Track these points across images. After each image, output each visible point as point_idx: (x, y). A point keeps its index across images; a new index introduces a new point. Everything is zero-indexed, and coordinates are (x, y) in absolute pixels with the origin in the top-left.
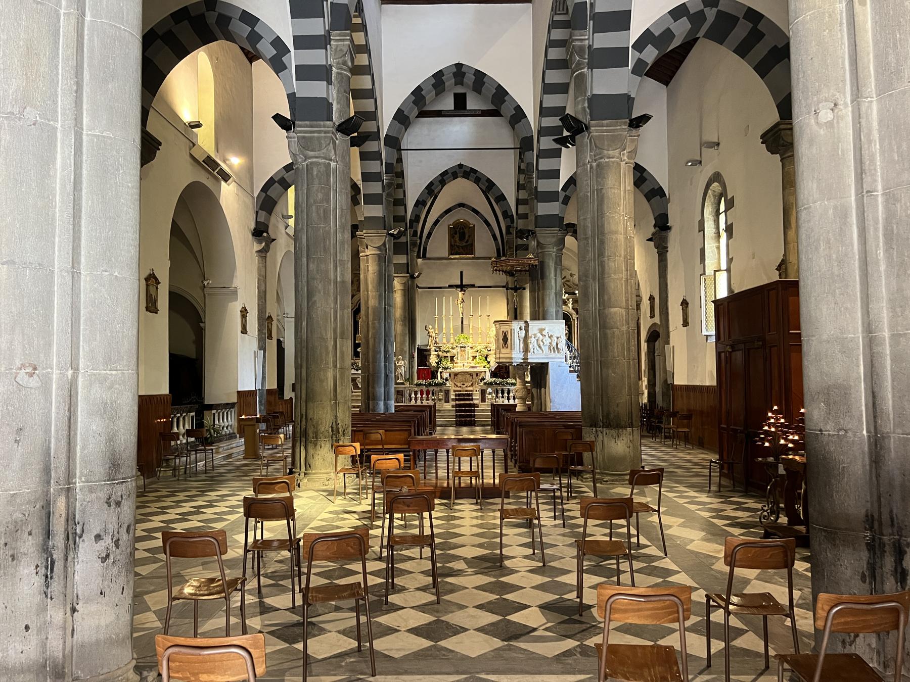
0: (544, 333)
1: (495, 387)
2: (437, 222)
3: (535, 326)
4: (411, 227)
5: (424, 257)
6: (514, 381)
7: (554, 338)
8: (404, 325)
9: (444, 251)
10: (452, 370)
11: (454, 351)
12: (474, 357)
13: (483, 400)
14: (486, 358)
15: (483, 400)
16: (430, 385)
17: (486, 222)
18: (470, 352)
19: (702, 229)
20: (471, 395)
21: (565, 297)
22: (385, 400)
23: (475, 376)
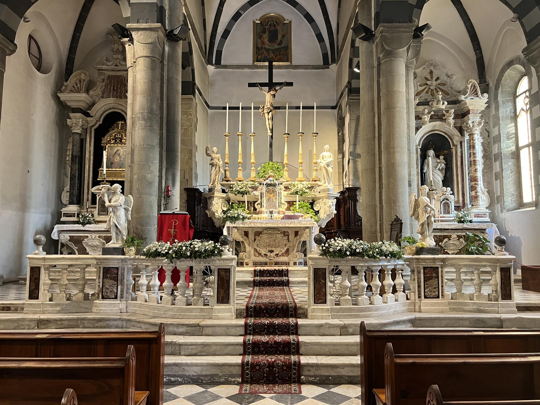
1: (352, 261)
2: (237, 16)
6: (395, 248)
8: (149, 127)
9: (248, 57)
10: (247, 224)
11: (257, 193)
12: (291, 204)
13: (320, 296)
14: (312, 204)
15: (320, 296)
16: (179, 255)
17: (309, 18)
18: (285, 196)
20: (285, 273)
21: (443, 106)
23: (292, 236)
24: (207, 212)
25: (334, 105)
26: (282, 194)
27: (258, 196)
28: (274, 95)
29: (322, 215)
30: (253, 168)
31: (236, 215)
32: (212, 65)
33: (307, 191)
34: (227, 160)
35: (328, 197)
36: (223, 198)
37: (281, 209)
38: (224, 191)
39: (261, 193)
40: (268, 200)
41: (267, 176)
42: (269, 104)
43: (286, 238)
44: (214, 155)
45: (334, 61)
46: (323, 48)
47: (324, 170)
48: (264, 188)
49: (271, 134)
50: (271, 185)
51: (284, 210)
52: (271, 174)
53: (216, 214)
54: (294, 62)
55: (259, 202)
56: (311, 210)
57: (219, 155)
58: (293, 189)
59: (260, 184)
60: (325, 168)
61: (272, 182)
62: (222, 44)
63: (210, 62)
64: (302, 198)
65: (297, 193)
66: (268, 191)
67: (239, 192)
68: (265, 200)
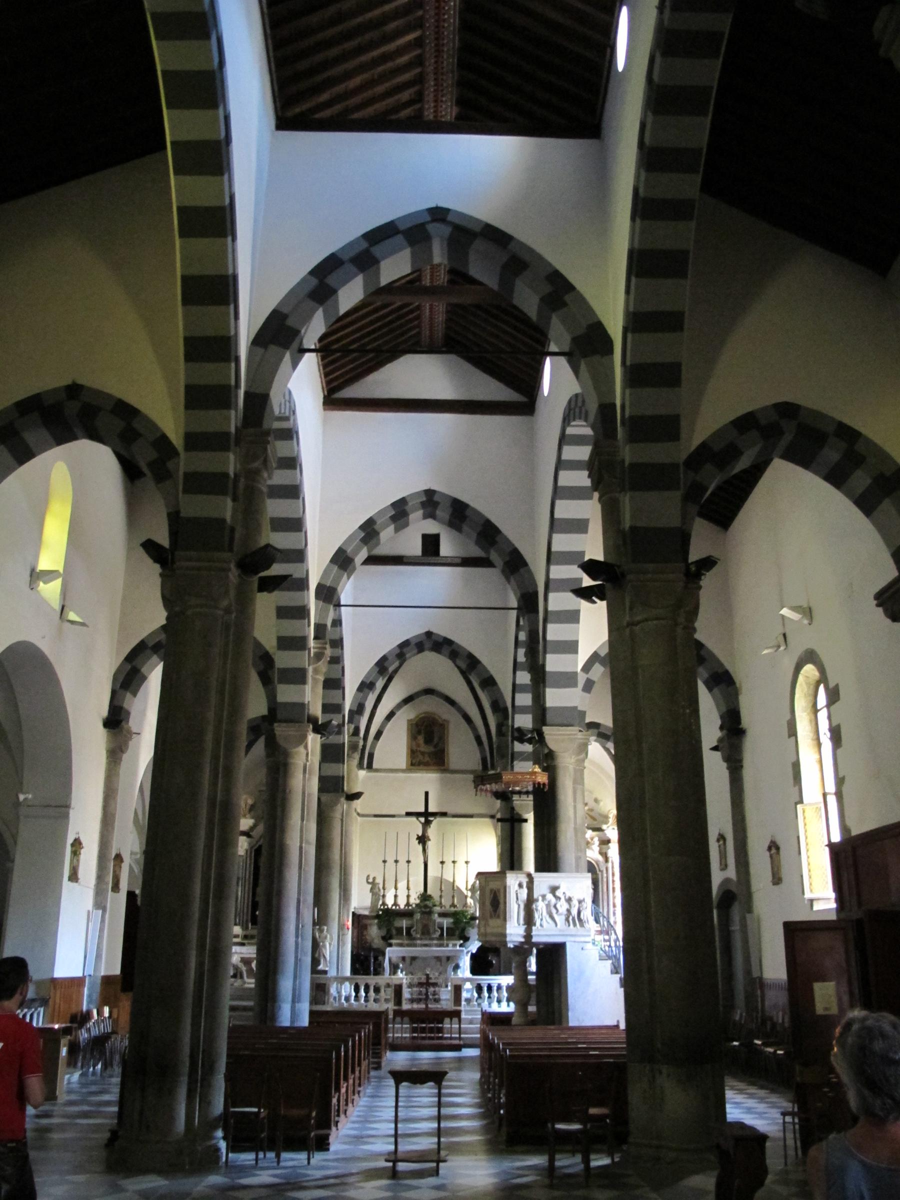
0: (558, 893)
3: (544, 881)
4: (350, 721)
5: (370, 766)
7: (575, 902)
9: (402, 760)
19: (792, 732)
22: (293, 1002)
43: (439, 963)
46: (482, 751)
62: (374, 746)
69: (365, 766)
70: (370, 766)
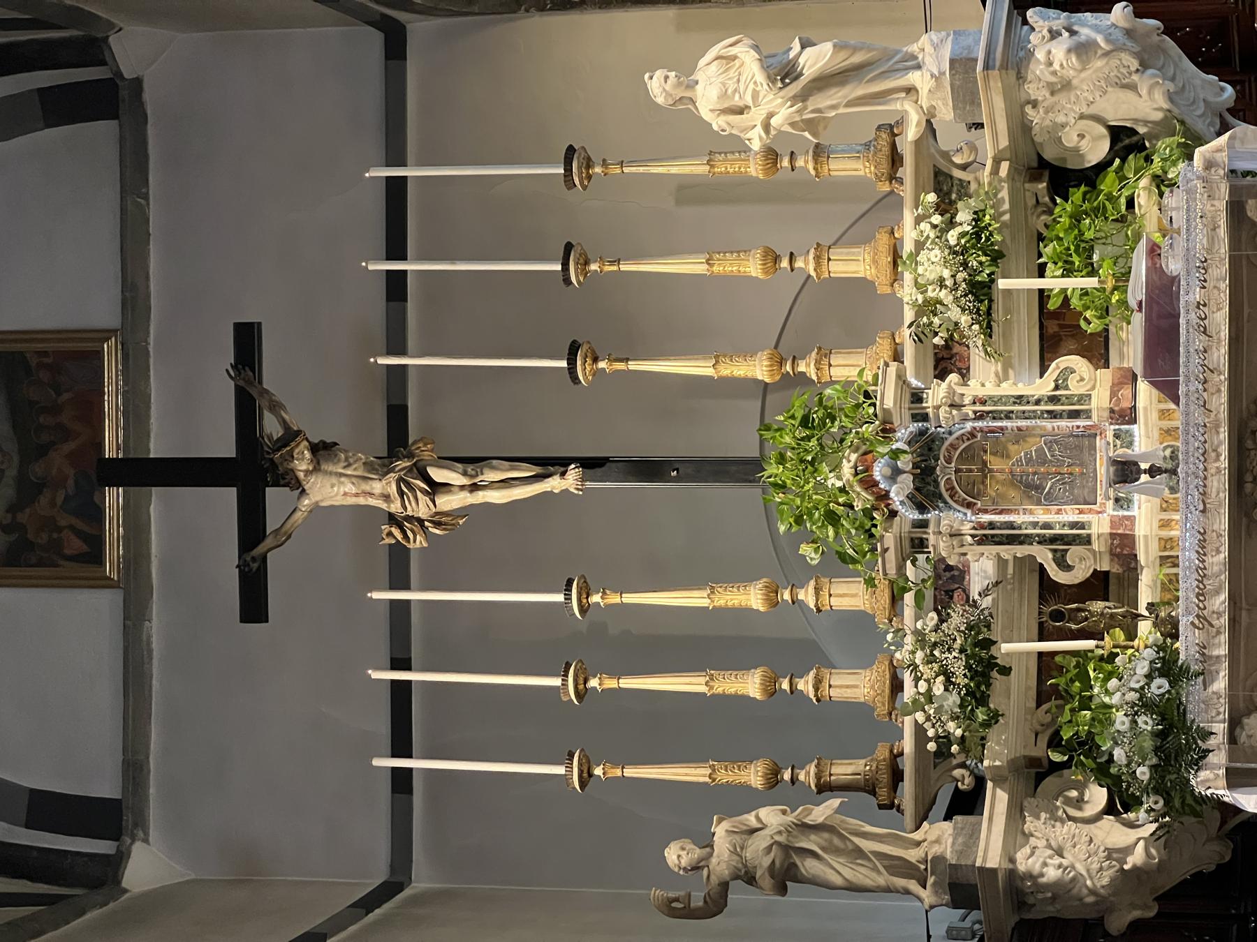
5: (111, 818)
9: (76, 619)
11: (982, 568)
12: (1058, 330)
14: (1060, 177)
24: (1117, 923)
25: (375, 40)
26: (990, 390)
27: (1001, 563)
28: (315, 449)
29: (1144, 104)
30: (807, 596)
31: (1146, 723)
32: (116, 863)
33: (964, 217)
34: (754, 776)
35: (1014, 61)
36: (1016, 812)
37: (1100, 400)
38: (967, 803)
39: (983, 541)
40: (1032, 490)
41: (862, 498)
42: (377, 487)
44: (722, 858)
45: (92, 49)
47: (822, 101)
48: (953, 520)
49: (573, 473)
50: (925, 476)
51: (1105, 377)
52: (847, 469)
53: (1137, 858)
54: (101, 311)
55: (1044, 556)
56: (1108, 183)
57: (721, 831)
58: (955, 313)
59: (919, 545)
60: (803, 96)
61: (905, 462)
63: (104, 876)
64: (1018, 254)
65: (980, 291)
66: (971, 497)
67: (977, 695)
68: (1030, 516)
69: (102, 847)
70: (111, 818)
